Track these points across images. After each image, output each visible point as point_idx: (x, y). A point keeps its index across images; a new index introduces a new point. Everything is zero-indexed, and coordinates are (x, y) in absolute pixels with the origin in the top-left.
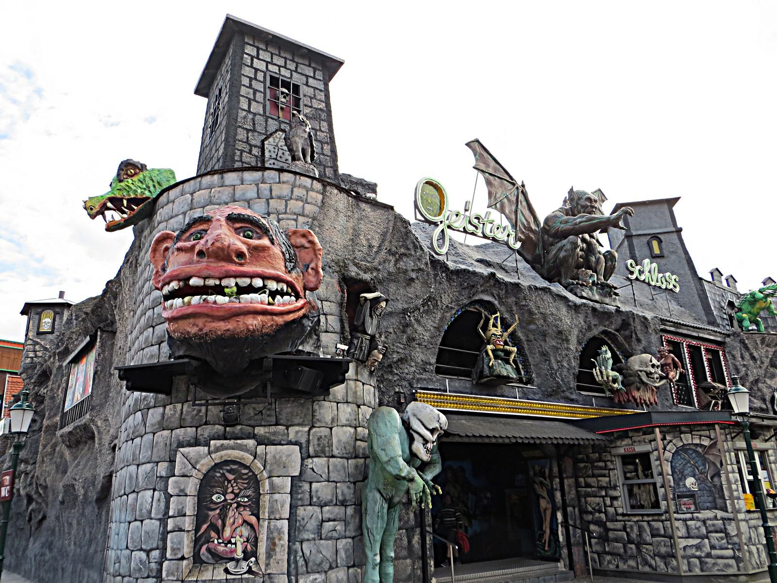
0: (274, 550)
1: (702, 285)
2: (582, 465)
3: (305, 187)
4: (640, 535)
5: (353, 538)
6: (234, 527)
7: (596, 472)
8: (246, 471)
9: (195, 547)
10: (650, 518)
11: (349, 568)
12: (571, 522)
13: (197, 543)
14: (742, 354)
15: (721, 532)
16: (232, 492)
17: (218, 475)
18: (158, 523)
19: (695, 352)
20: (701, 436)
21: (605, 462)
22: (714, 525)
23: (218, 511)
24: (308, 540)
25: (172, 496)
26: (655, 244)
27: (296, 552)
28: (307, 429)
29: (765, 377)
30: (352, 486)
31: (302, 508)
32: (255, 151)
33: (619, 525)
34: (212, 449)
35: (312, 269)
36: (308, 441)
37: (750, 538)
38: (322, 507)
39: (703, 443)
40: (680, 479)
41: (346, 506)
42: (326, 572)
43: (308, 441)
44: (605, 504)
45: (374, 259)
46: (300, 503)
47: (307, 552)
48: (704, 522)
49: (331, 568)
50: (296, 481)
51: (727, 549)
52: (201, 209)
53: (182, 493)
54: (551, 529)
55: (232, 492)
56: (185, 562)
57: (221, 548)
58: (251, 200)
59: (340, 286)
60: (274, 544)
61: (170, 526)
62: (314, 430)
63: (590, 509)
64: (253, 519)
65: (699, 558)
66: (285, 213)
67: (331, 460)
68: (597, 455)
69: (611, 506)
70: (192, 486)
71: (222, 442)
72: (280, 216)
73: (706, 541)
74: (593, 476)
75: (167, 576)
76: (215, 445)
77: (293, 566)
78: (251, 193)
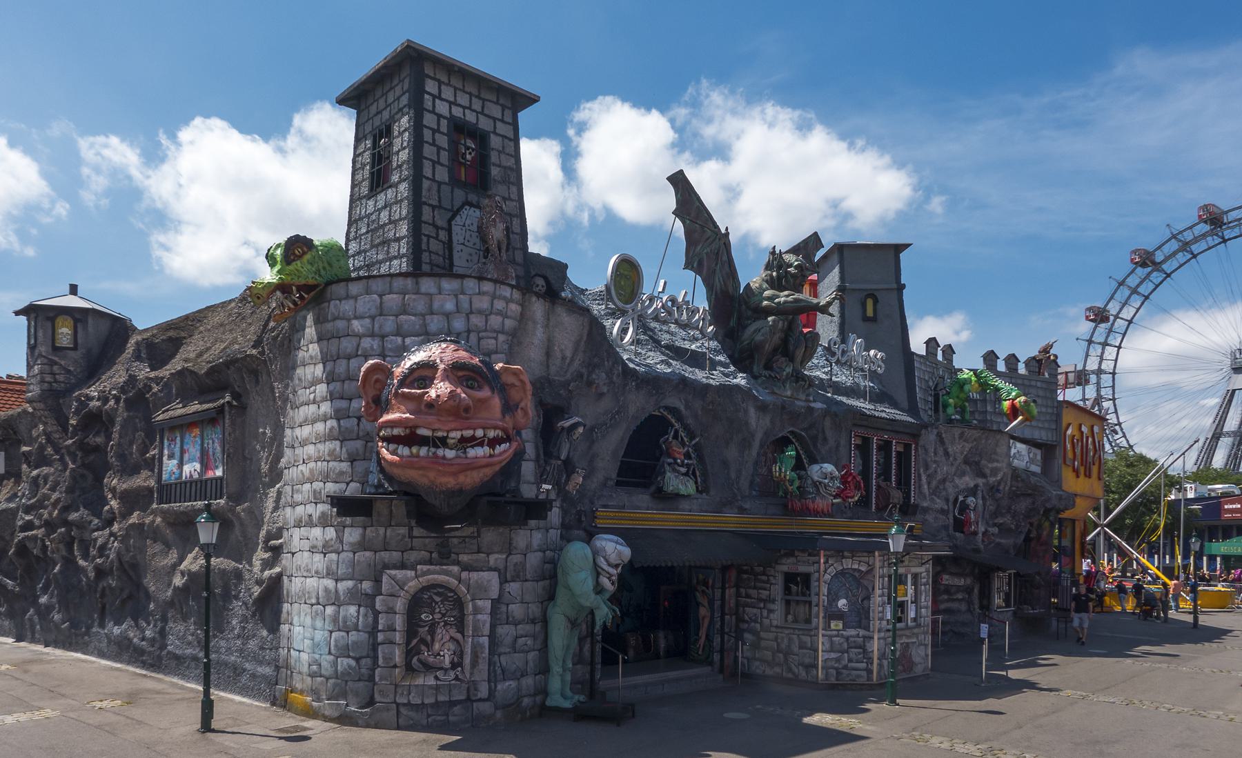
0: (477, 661)
1: (912, 361)
2: (745, 576)
3: (505, 298)
4: (789, 646)
5: (539, 650)
6: (442, 642)
7: (759, 585)
8: (452, 594)
9: (406, 658)
10: (801, 632)
11: (536, 675)
12: (726, 630)
13: (409, 653)
14: (935, 449)
15: (860, 648)
16: (440, 612)
17: (426, 596)
18: (367, 635)
19: (885, 447)
20: (860, 562)
21: (768, 576)
22: (855, 642)
23: (427, 628)
24: (505, 653)
25: (380, 613)
26: (870, 303)
27: (495, 663)
28: (504, 556)
29: (954, 475)
30: (540, 605)
31: (500, 626)
32: (443, 235)
33: (771, 636)
34: (419, 572)
35: (522, 409)
36: (506, 568)
37: (885, 653)
38: (516, 625)
39: (861, 568)
40: (834, 600)
41: (535, 623)
42: (519, 679)
43: (506, 568)
44: (762, 615)
45: (566, 372)
46: (498, 622)
47: (504, 664)
48: (847, 639)
49: (522, 676)
50: (496, 603)
51: (863, 662)
52: (394, 318)
53: (391, 611)
54: (707, 636)
55: (440, 612)
56: (397, 670)
57: (431, 659)
58: (450, 314)
59: (537, 411)
60: (477, 657)
61: (380, 637)
62: (511, 557)
63: (746, 618)
64: (459, 636)
65: (836, 669)
66: (486, 330)
67: (525, 583)
68: (762, 569)
69: (767, 618)
70: (400, 605)
71: (428, 567)
72: (481, 334)
73: (846, 655)
74: (755, 588)
75: (380, 680)
76: (422, 570)
77: (493, 674)
78: (450, 306)
